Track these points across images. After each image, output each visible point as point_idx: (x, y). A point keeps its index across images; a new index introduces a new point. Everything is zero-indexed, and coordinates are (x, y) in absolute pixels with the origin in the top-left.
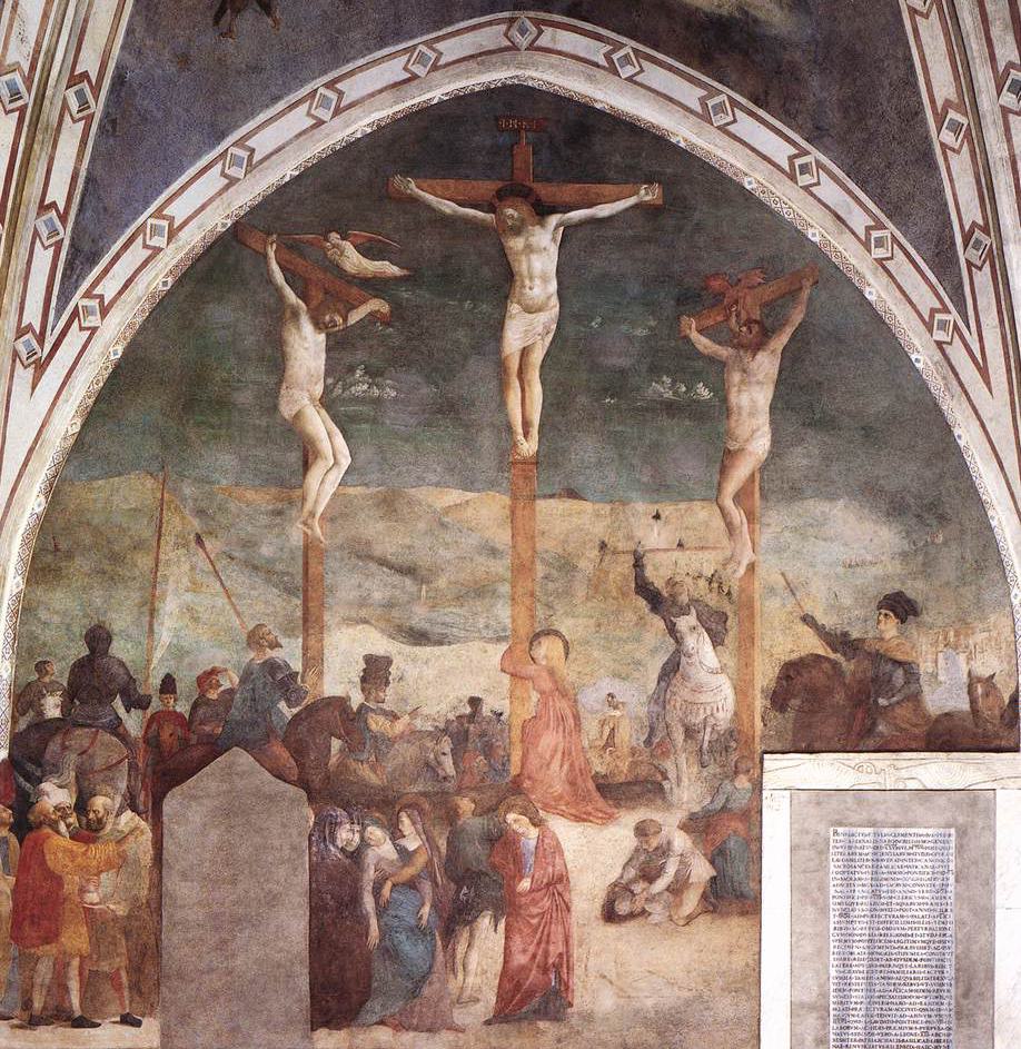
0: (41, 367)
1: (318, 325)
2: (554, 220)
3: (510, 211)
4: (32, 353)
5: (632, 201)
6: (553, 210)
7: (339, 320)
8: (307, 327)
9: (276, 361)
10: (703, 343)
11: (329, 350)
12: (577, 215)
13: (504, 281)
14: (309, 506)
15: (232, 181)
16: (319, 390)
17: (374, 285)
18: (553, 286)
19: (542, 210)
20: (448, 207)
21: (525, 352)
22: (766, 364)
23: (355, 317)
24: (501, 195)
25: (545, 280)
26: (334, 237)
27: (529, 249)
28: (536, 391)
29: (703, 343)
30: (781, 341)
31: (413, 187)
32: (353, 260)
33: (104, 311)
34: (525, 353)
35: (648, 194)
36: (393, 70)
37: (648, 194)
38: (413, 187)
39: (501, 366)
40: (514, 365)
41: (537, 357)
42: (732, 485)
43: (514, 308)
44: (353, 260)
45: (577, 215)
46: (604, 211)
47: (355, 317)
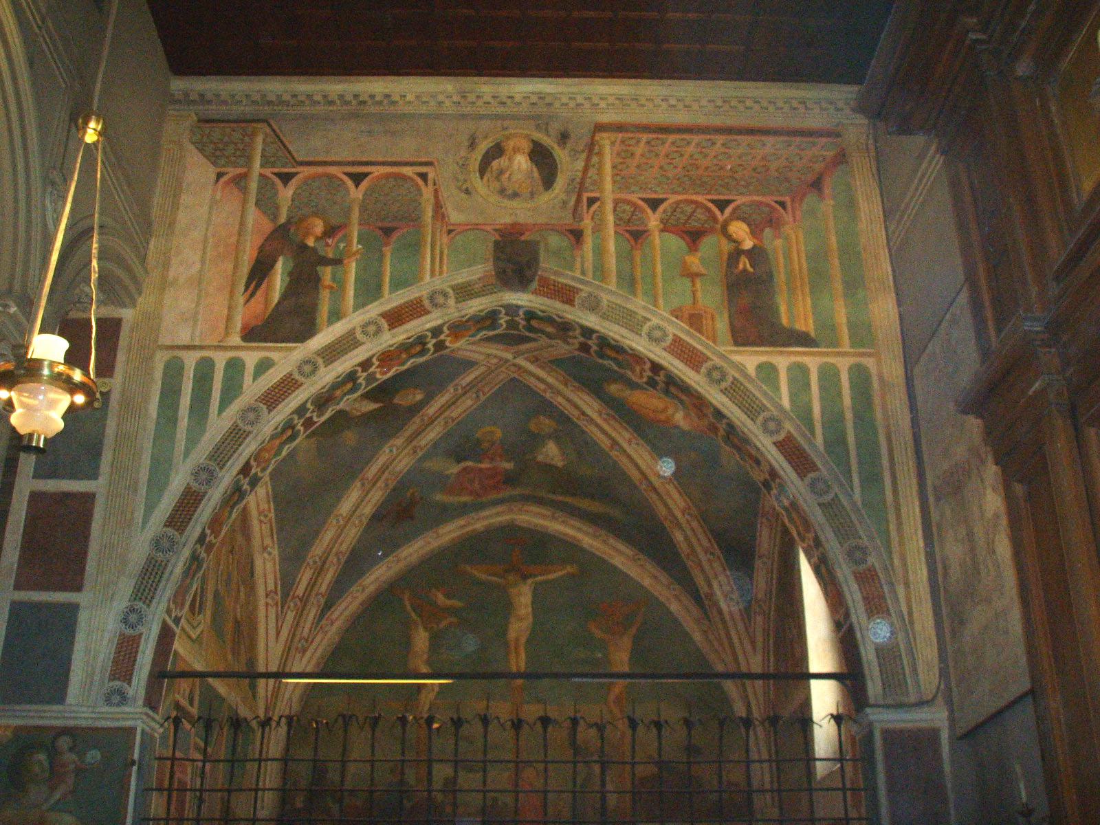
0: (304, 651)
1: (426, 628)
2: (530, 581)
3: (510, 578)
4: (303, 646)
5: (564, 572)
6: (531, 576)
7: (435, 626)
8: (421, 630)
9: (407, 643)
10: (598, 634)
11: (431, 638)
12: (540, 578)
13: (507, 607)
14: (420, 708)
15: (389, 568)
16: (425, 657)
17: (449, 611)
18: (530, 609)
19: (525, 577)
20: (483, 576)
21: (517, 639)
22: (626, 642)
23: (443, 624)
24: (506, 571)
25: (526, 606)
26: (433, 590)
27: (519, 594)
28: (523, 656)
29: (598, 634)
30: (633, 630)
31: (468, 568)
32: (441, 599)
33: (332, 624)
34: (517, 639)
35: (570, 569)
36: (462, 522)
37: (570, 569)
38: (468, 568)
39: (506, 645)
40: (512, 645)
41: (523, 640)
42: (612, 697)
43: (512, 620)
44: (441, 599)
45: (540, 578)
46: (550, 577)
47: (443, 624)
